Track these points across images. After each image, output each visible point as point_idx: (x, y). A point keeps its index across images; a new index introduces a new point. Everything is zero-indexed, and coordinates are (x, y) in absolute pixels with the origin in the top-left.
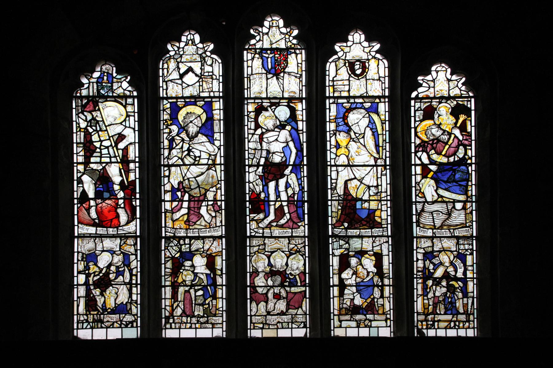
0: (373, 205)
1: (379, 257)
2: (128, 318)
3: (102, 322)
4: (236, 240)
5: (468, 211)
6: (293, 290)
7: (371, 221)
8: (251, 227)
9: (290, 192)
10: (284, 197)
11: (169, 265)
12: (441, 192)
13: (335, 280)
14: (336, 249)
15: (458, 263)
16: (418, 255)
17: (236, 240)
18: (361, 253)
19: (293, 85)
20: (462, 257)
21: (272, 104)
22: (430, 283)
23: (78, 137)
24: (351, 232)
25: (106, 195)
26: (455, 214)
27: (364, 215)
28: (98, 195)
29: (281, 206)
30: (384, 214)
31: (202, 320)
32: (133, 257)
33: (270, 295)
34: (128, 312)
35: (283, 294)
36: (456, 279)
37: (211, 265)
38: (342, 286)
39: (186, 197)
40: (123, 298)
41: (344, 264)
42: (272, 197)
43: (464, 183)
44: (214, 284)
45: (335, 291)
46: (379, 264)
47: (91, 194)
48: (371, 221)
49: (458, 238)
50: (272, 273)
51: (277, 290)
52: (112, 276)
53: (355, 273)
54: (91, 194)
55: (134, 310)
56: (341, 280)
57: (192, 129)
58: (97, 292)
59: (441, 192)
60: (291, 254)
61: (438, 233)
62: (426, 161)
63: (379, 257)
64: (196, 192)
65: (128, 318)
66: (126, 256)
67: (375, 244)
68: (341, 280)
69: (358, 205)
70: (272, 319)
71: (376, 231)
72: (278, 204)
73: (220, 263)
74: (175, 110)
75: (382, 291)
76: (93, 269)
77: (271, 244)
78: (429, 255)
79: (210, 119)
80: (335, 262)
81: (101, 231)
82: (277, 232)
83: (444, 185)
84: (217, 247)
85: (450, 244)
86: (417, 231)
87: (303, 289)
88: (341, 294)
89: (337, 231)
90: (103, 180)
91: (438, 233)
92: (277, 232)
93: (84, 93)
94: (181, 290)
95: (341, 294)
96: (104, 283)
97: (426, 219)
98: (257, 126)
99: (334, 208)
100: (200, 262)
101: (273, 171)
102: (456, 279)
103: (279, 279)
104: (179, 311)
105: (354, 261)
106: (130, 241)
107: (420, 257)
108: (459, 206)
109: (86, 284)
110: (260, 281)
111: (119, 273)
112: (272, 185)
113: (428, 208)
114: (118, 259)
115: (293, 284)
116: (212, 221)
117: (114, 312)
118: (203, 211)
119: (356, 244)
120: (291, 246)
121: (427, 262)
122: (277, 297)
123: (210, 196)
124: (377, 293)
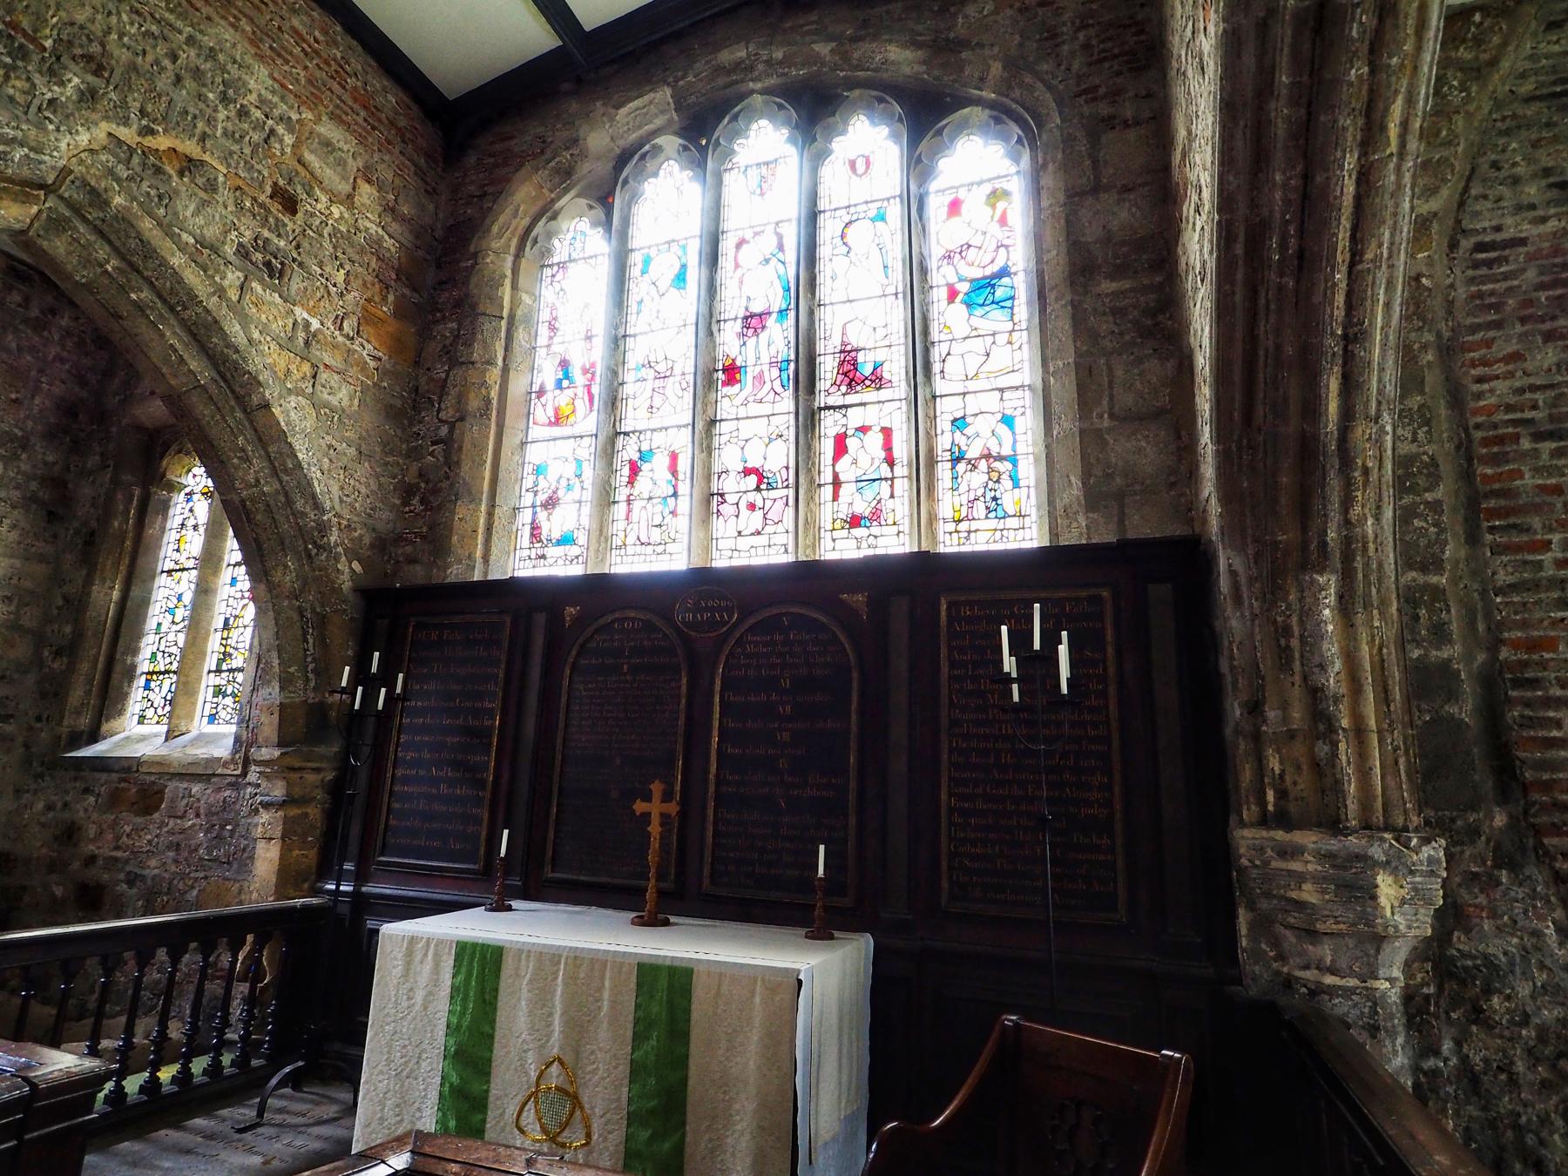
0: (880, 355)
1: (887, 432)
2: (575, 551)
3: (543, 557)
4: (707, 428)
5: (1016, 346)
6: (773, 494)
7: (877, 380)
8: (725, 408)
9: (773, 353)
10: (765, 359)
11: (626, 471)
12: (975, 321)
13: (827, 477)
14: (830, 425)
15: (1003, 430)
16: (944, 424)
17: (707, 428)
18: (864, 429)
19: (787, 204)
20: (1007, 420)
21: (756, 234)
22: (961, 467)
23: (545, 315)
24: (850, 399)
25: (565, 383)
26: (995, 352)
27: (867, 370)
28: (559, 385)
29: (761, 374)
30: (896, 367)
31: (660, 549)
32: (585, 464)
33: (743, 505)
34: (573, 542)
35: (759, 503)
36: (1000, 458)
37: (673, 470)
38: (837, 483)
39: (651, 374)
40: (570, 525)
41: (841, 447)
42: (751, 361)
43: (1008, 304)
44: (675, 495)
45: (827, 492)
46: (888, 446)
47: (550, 385)
48: (877, 380)
49: (1002, 390)
50: (747, 472)
51: (752, 497)
52: (560, 493)
53: (855, 462)
54: (550, 385)
55: (582, 540)
56: (836, 476)
57: (664, 283)
58: (542, 515)
59: (975, 321)
60: (771, 440)
61: (971, 386)
62: (953, 279)
63: (887, 432)
64: (661, 368)
65: (575, 551)
66: (579, 462)
67: (885, 409)
68: (836, 476)
69: (860, 359)
70: (743, 543)
71: (884, 394)
72: (758, 369)
73: (684, 465)
74: (647, 261)
75: (892, 486)
76: (542, 484)
77: (747, 428)
78: (958, 423)
79: (684, 266)
80: (827, 447)
81: (556, 431)
82: (754, 409)
83: (979, 311)
84: (682, 440)
85: (991, 402)
86: (940, 386)
87: (785, 492)
88: (835, 497)
89: (831, 401)
90: (564, 364)
91: (971, 386)
92: (754, 409)
93: (556, 260)
94: (637, 505)
95: (835, 497)
96: (551, 503)
97: (953, 366)
98: (737, 266)
99: (828, 367)
100: (660, 462)
101: (753, 322)
102: (1000, 458)
103: (753, 479)
104: (631, 539)
105: (851, 443)
106: (587, 441)
107: (947, 426)
108: (1002, 339)
109: (533, 506)
110: (730, 485)
111: (569, 488)
112: (751, 342)
113: (957, 348)
114: (569, 470)
115: (770, 487)
116: (678, 407)
117: (559, 543)
118: (668, 392)
119: (856, 417)
120: (771, 429)
121: (958, 434)
122: (752, 507)
123: (677, 371)
124: (885, 486)
